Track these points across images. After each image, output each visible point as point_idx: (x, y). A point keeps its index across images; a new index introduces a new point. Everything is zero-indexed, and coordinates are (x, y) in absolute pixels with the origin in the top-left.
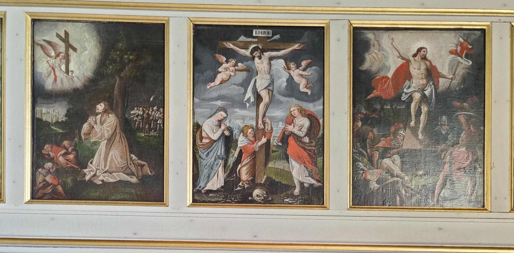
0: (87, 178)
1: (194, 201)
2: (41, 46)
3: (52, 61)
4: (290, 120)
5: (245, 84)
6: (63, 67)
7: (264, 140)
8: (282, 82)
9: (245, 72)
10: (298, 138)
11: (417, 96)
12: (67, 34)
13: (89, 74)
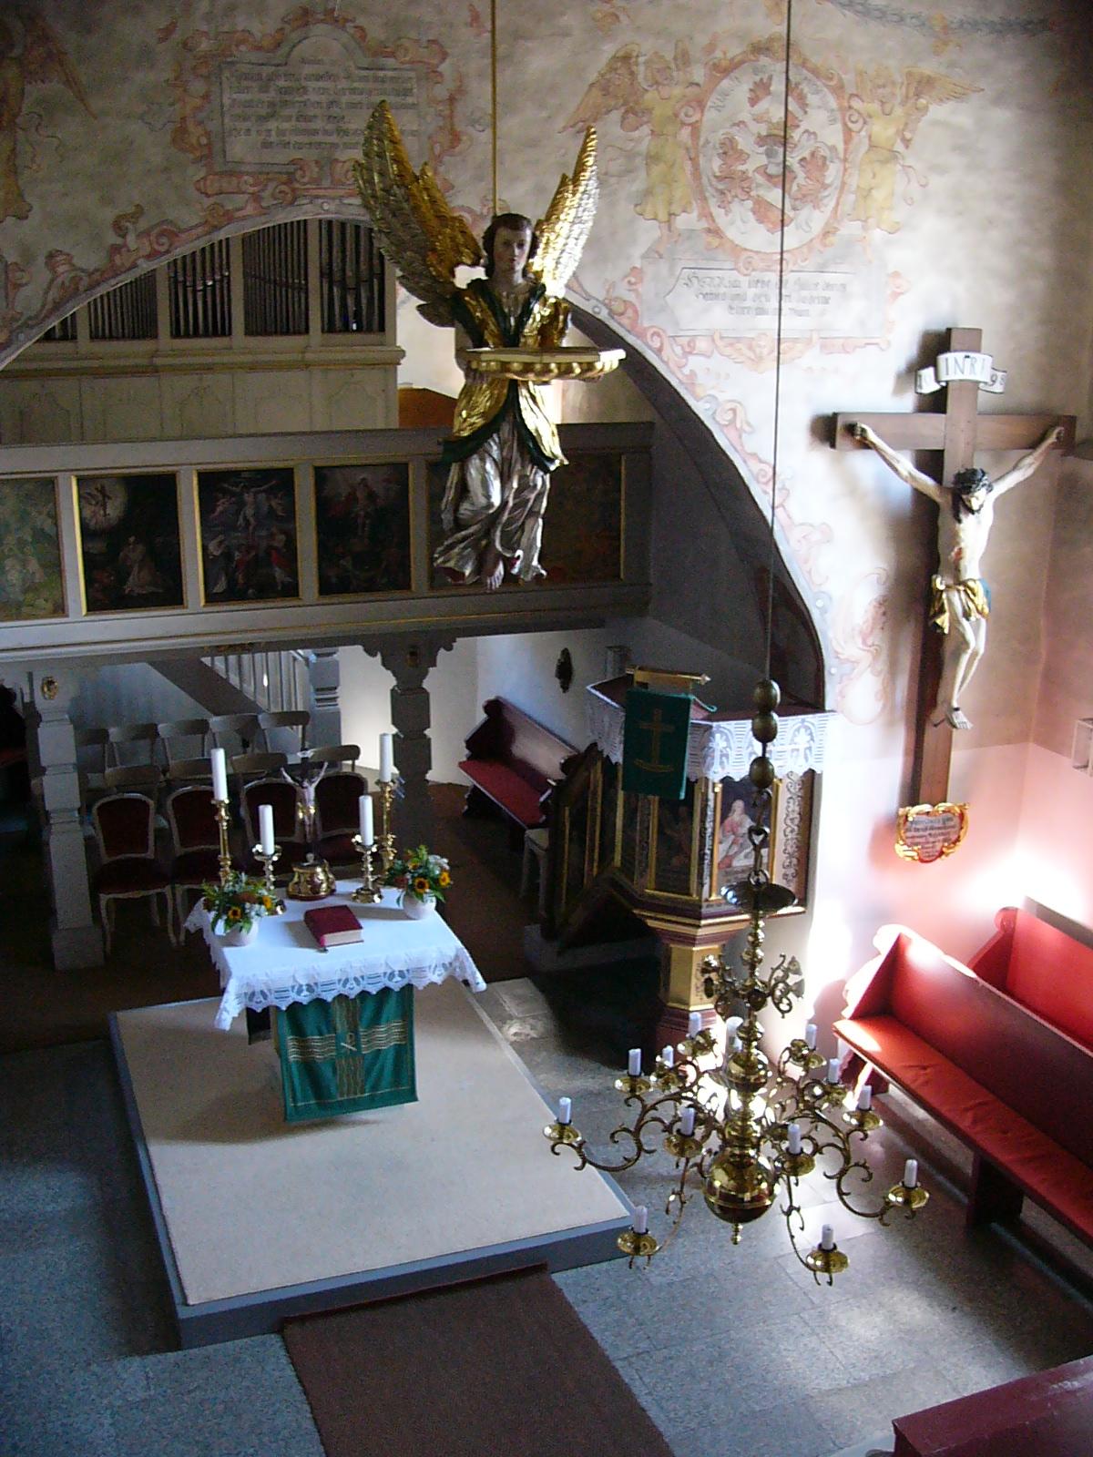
0: (127, 592)
1: (206, 602)
2: (85, 498)
3: (93, 508)
4: (272, 536)
5: (238, 513)
6: (102, 512)
7: (253, 554)
8: (265, 509)
9: (378, 768)
10: (276, 549)
11: (362, 513)
12: (103, 487)
13: (121, 515)
